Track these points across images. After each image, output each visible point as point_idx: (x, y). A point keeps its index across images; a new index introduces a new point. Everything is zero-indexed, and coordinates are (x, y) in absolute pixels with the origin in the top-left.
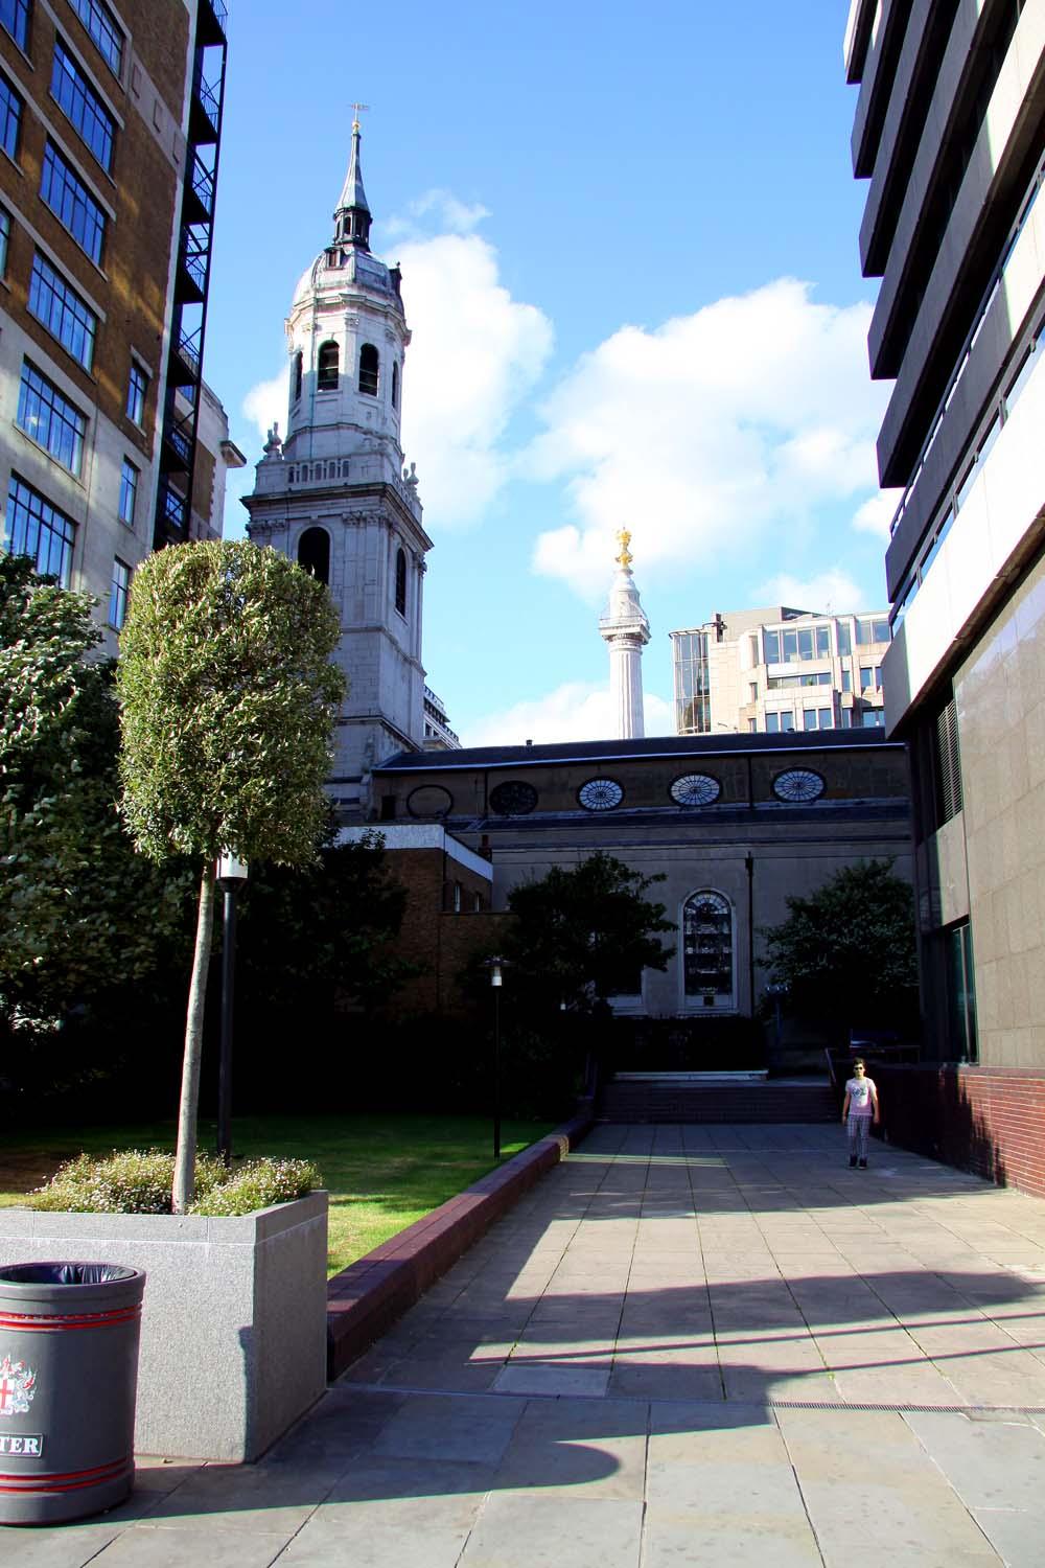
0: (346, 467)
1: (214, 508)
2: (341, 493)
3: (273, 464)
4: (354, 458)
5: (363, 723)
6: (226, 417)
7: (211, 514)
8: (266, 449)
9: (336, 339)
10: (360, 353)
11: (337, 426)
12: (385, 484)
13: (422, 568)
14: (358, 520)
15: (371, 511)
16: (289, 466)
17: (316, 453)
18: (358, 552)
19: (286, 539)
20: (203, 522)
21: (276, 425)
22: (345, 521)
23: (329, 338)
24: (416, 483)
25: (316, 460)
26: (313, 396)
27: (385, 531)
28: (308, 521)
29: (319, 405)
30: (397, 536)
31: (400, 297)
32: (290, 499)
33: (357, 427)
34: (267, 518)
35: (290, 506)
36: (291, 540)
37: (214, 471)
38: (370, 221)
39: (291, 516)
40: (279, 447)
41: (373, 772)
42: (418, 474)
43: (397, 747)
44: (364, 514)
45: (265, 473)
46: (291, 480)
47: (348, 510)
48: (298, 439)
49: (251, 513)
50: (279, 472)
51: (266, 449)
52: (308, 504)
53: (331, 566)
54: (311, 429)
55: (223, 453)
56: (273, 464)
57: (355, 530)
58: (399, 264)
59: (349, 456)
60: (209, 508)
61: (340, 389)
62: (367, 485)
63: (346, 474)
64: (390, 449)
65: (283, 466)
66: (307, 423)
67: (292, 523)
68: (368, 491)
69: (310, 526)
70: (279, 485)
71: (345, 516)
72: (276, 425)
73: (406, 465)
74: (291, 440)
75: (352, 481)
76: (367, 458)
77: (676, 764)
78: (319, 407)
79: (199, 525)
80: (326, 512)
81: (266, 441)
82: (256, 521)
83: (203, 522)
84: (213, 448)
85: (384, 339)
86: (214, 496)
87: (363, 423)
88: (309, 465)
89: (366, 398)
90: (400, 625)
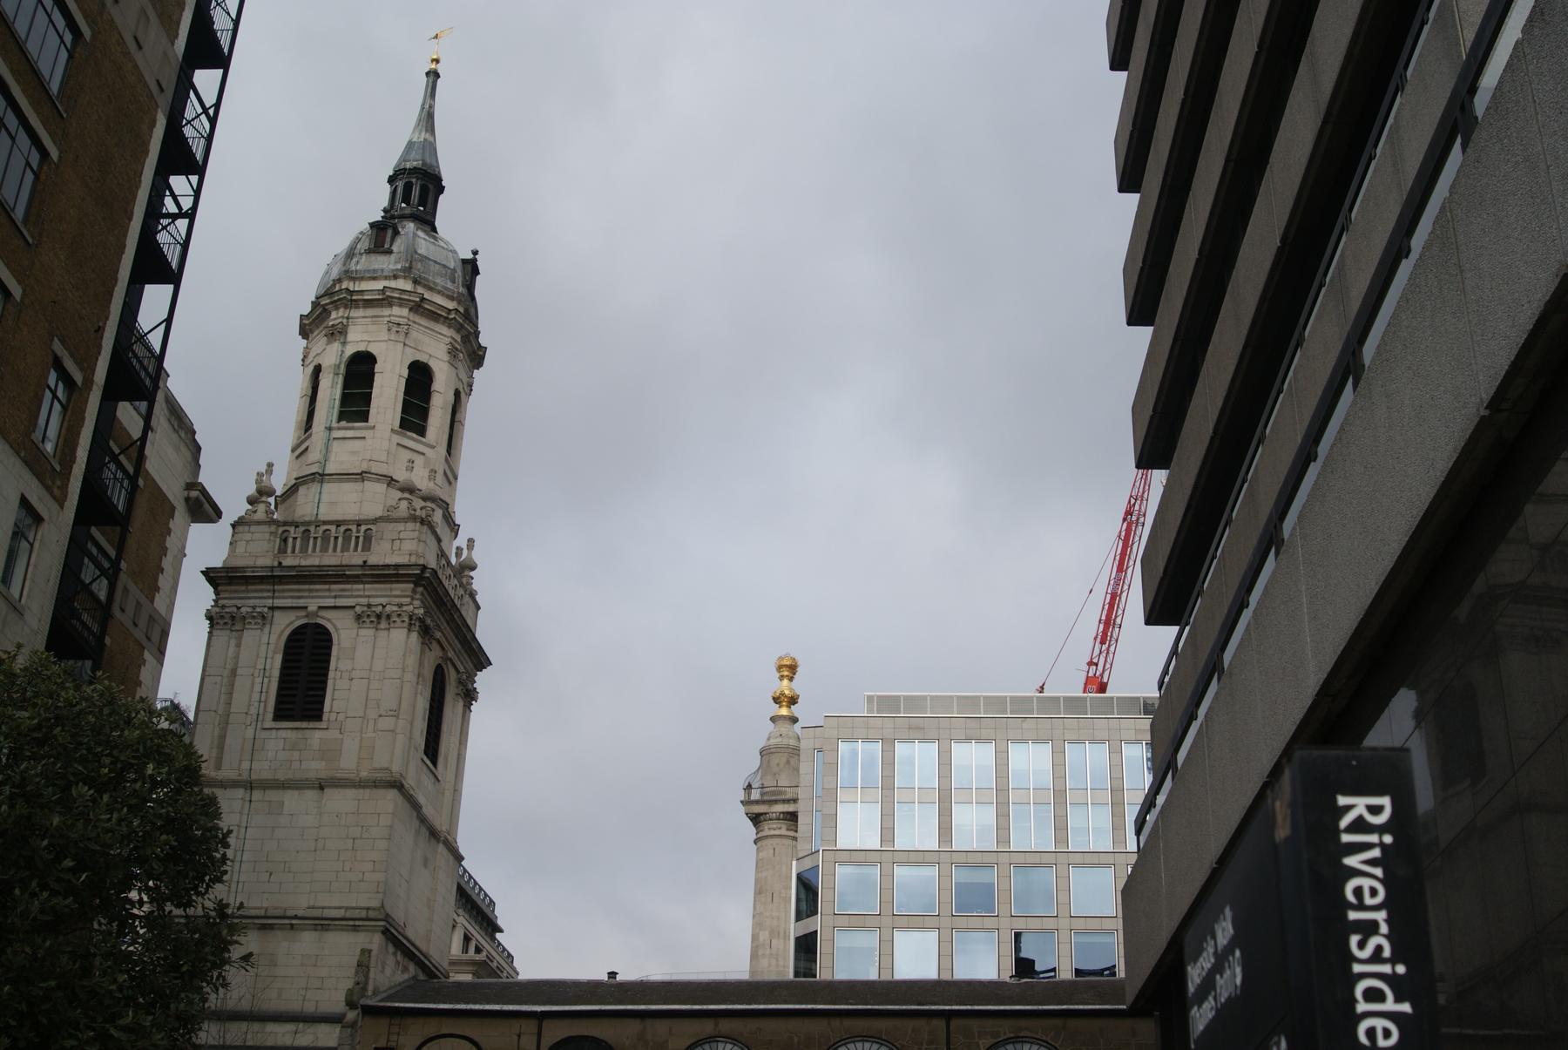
0: (368, 539)
1: (163, 581)
2: (357, 576)
3: (259, 523)
4: (382, 525)
5: (355, 928)
6: (199, 449)
7: (157, 589)
8: (251, 501)
9: (373, 349)
10: (405, 373)
11: (362, 476)
12: (424, 568)
13: (469, 696)
14: (379, 617)
15: (400, 605)
16: (281, 530)
17: (325, 513)
18: (375, 665)
19: (265, 639)
20: (143, 600)
21: (270, 465)
22: (358, 617)
23: (362, 348)
24: (473, 568)
25: (325, 523)
26: (330, 429)
27: (414, 636)
28: (303, 613)
29: (336, 443)
30: (435, 645)
31: (473, 299)
32: (275, 578)
33: (391, 481)
34: (239, 603)
36: (274, 638)
37: (171, 525)
38: (441, 189)
39: (278, 603)
40: (272, 500)
41: (363, 1007)
42: (477, 556)
43: (406, 969)
44: (388, 608)
45: (248, 536)
46: (282, 551)
47: (364, 601)
48: (302, 490)
49: (217, 593)
50: (267, 536)
51: (251, 501)
53: (330, 682)
54: (320, 477)
55: (187, 499)
56: (259, 523)
57: (371, 632)
58: (475, 253)
59: (375, 521)
60: (156, 580)
62: (397, 566)
63: (367, 548)
64: (438, 517)
65: (273, 528)
66: (314, 469)
67: (277, 614)
68: (397, 575)
69: (304, 621)
70: (260, 552)
71: (358, 609)
72: (270, 465)
73: (461, 541)
74: (292, 491)
75: (373, 559)
76: (401, 526)
77: (836, 1023)
78: (336, 446)
79: (138, 605)
80: (330, 602)
81: (251, 489)
82: (223, 607)
83: (143, 600)
84: (173, 490)
85: (446, 357)
86: (166, 563)
87: (401, 475)
88: (312, 529)
89: (410, 440)
90: (427, 780)
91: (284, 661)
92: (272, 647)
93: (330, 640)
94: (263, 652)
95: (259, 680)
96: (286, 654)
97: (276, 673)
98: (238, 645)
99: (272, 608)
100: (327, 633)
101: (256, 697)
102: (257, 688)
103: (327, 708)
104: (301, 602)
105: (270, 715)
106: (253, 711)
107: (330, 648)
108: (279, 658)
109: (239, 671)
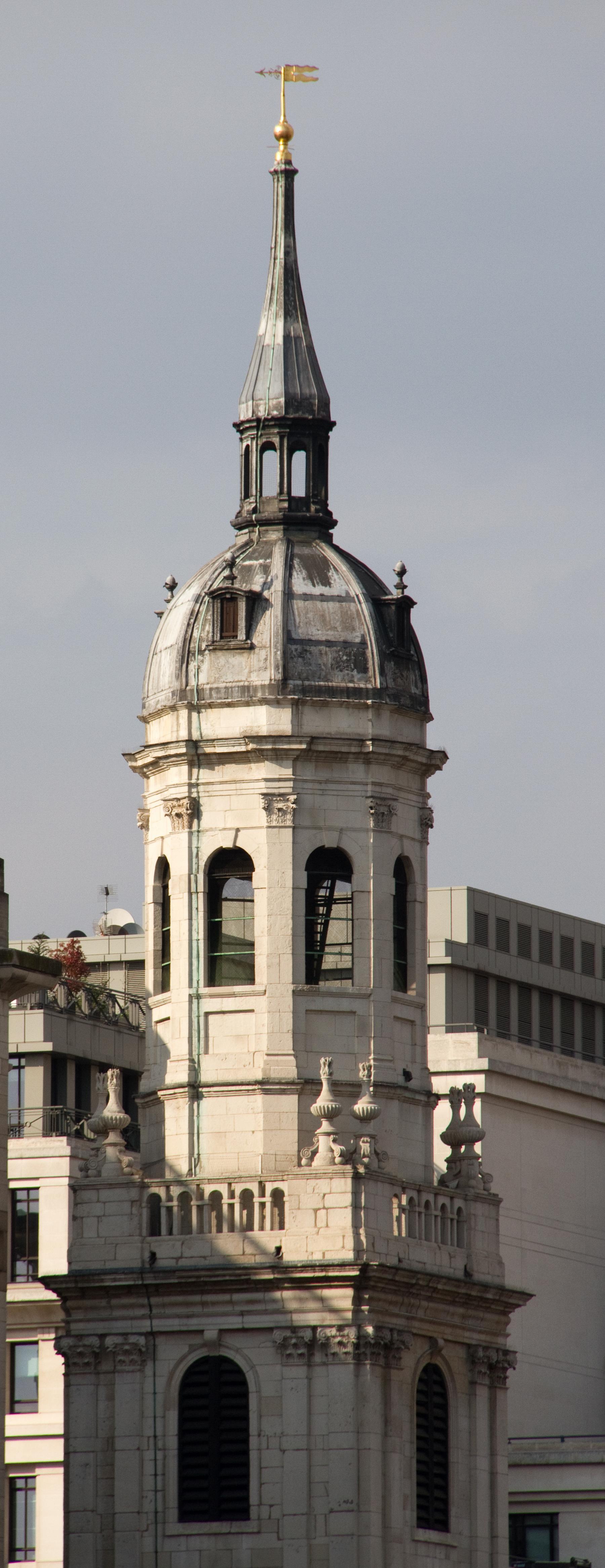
19: (149, 1387)
22: (283, 1346)
35: (154, 1300)
36: (161, 1382)
39: (159, 1325)
45: (97, 1209)
50: (126, 1206)
52: (197, 1298)
53: (253, 1455)
61: (258, 987)
67: (160, 1340)
82: (80, 1337)
91: (183, 1420)
92: (160, 1398)
93: (244, 1383)
94: (150, 1404)
95: (149, 1455)
96: (183, 1409)
97: (173, 1442)
98: (111, 1398)
99: (152, 1334)
100: (238, 1371)
101: (149, 1483)
102: (149, 1469)
103: (253, 1499)
104: (194, 1324)
105: (173, 1513)
106: (149, 1507)
107: (245, 1395)
108: (173, 1416)
109: (119, 1444)
